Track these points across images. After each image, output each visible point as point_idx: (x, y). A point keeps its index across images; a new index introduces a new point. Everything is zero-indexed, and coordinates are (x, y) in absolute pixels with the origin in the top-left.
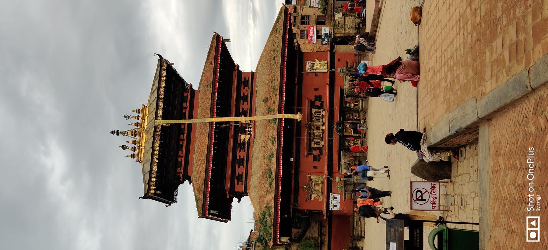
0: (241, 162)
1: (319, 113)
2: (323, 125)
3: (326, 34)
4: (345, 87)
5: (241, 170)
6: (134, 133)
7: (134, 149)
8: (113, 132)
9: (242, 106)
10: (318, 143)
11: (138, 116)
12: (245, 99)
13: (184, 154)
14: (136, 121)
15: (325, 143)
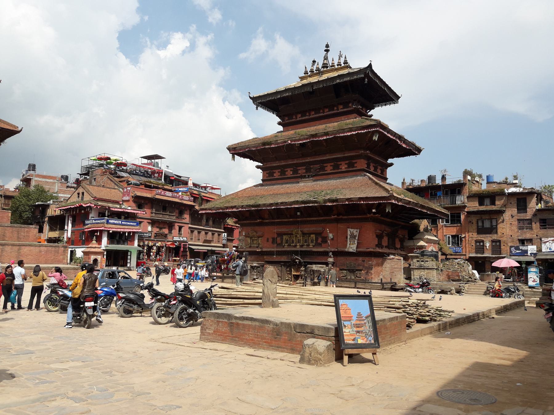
0: (283, 173)
1: (312, 242)
2: (302, 246)
3: (526, 251)
4: (314, 266)
5: (277, 175)
6: (325, 66)
7: (312, 71)
8: (327, 46)
9: (329, 165)
10: (287, 241)
11: (334, 66)
12: (336, 167)
13: (298, 119)
14: (336, 64)
15: (286, 248)
